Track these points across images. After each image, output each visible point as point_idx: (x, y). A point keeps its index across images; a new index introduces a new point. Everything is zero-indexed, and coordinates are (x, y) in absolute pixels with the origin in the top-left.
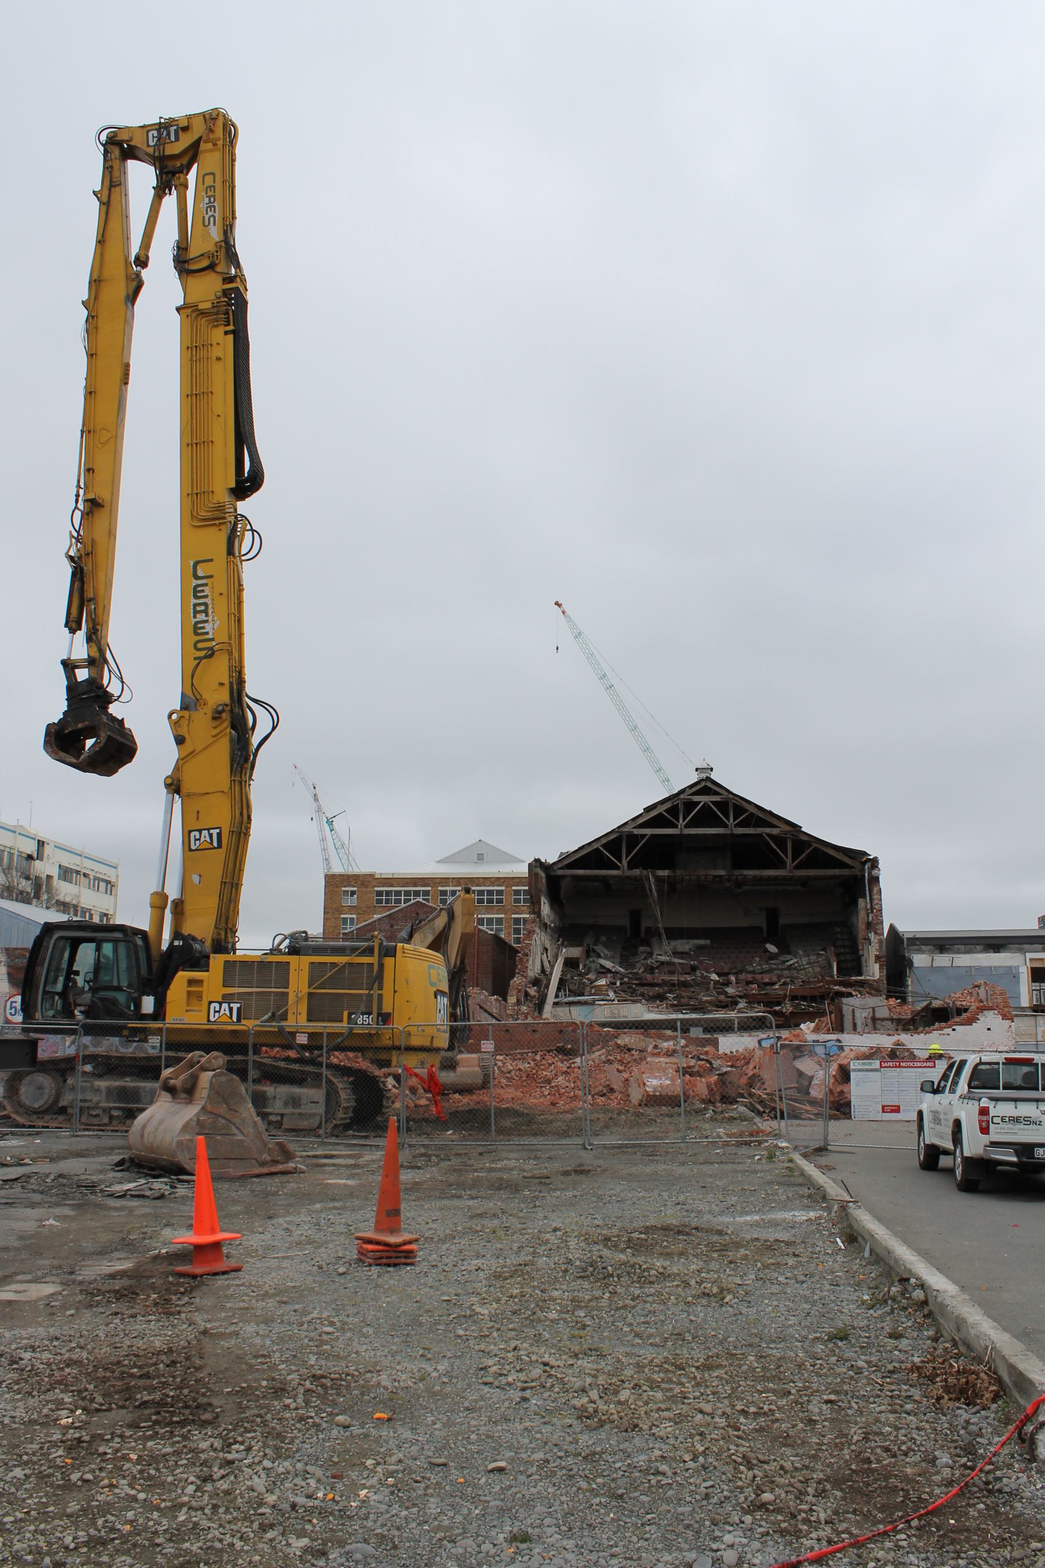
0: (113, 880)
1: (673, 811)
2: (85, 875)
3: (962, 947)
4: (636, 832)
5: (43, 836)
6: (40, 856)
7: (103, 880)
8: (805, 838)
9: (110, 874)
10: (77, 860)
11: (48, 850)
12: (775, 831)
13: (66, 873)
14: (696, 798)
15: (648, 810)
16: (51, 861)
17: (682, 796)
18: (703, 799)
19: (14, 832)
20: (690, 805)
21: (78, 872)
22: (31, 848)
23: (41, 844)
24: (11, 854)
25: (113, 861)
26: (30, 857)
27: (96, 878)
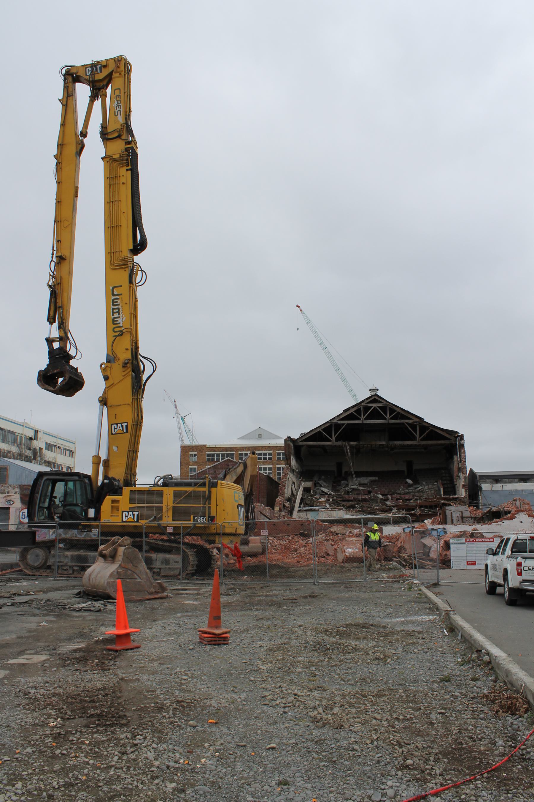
0: (73, 450)
1: (358, 411)
2: (59, 447)
3: (507, 480)
4: (339, 422)
5: (37, 428)
6: (36, 438)
7: (68, 450)
8: (426, 425)
9: (71, 447)
10: (55, 440)
11: (40, 435)
12: (411, 421)
13: (49, 447)
14: (370, 405)
16: (42, 440)
17: (363, 404)
18: (374, 405)
19: (23, 426)
20: (367, 409)
21: (55, 446)
22: (31, 434)
23: (36, 432)
24: (21, 437)
25: (73, 440)
26: (31, 439)
27: (64, 449)
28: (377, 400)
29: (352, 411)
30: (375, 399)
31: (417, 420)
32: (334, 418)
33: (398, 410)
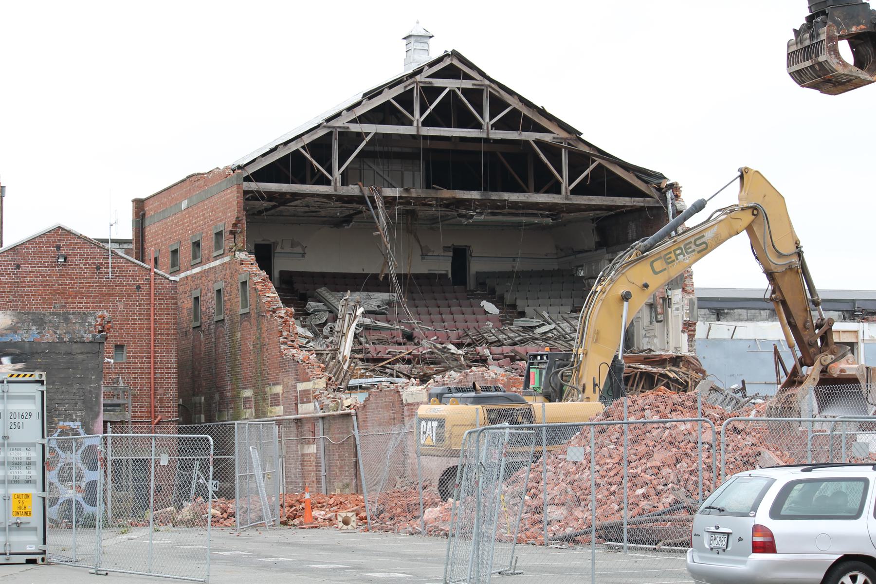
1: (405, 99)
3: (743, 312)
4: (355, 128)
8: (586, 149)
12: (547, 138)
14: (438, 83)
15: (371, 95)
17: (418, 78)
18: (450, 84)
20: (430, 92)
28: (460, 70)
29: (388, 96)
30: (451, 64)
31: (564, 134)
32: (339, 115)
33: (514, 103)
